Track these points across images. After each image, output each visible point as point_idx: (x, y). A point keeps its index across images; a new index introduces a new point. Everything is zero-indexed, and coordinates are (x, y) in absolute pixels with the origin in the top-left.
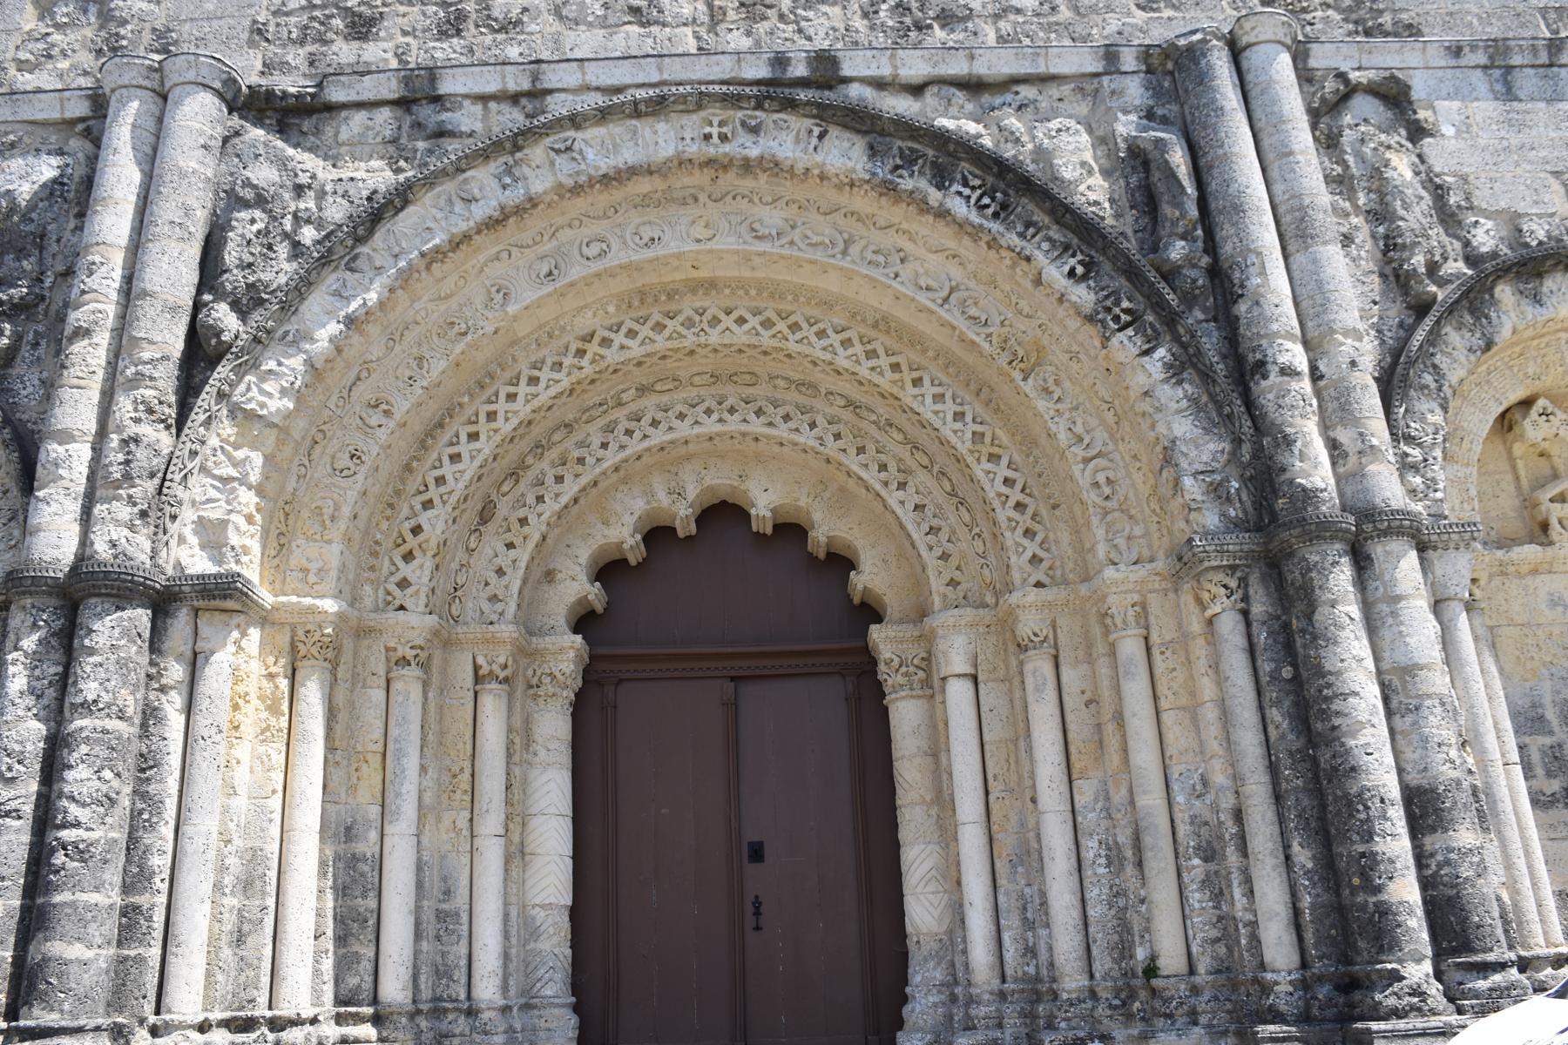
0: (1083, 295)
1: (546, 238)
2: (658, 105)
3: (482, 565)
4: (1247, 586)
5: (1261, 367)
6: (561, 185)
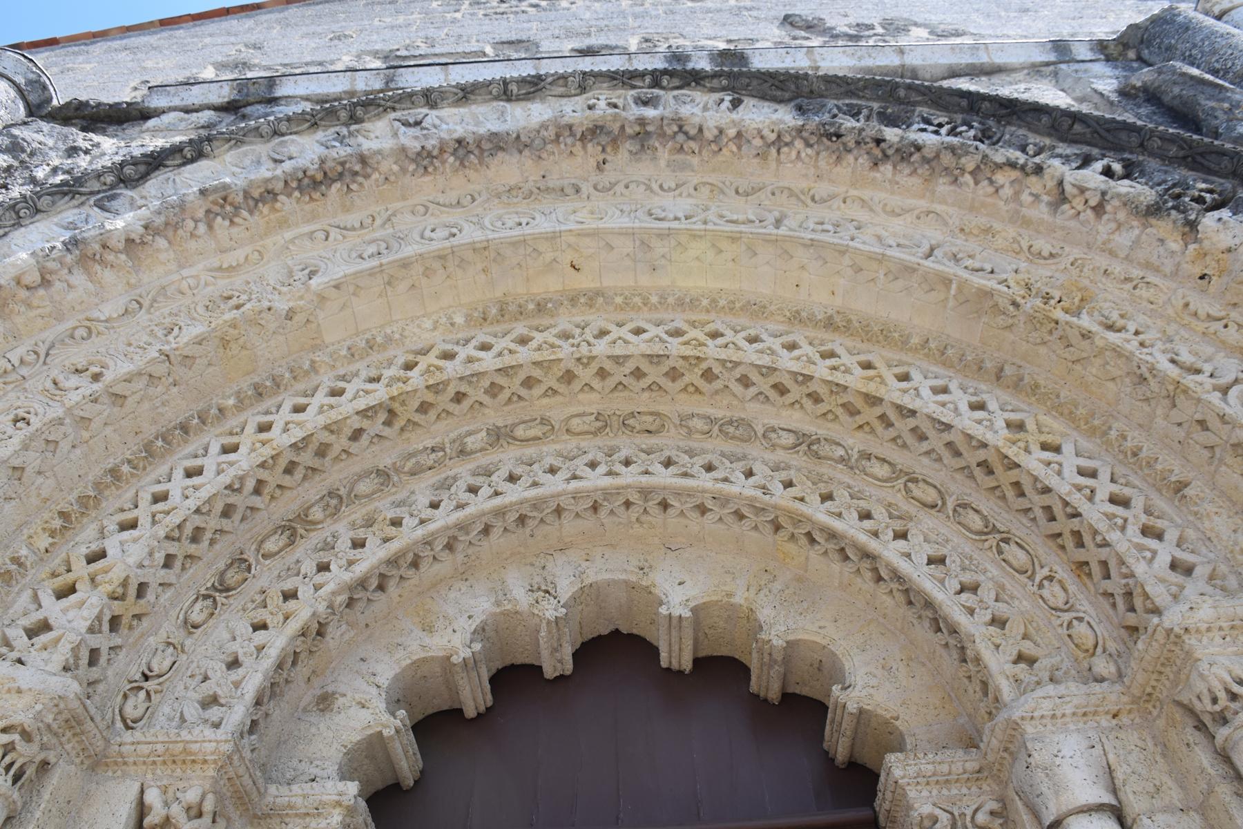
0: (1141, 191)
1: (378, 222)
3: (205, 652)
6: (403, 149)
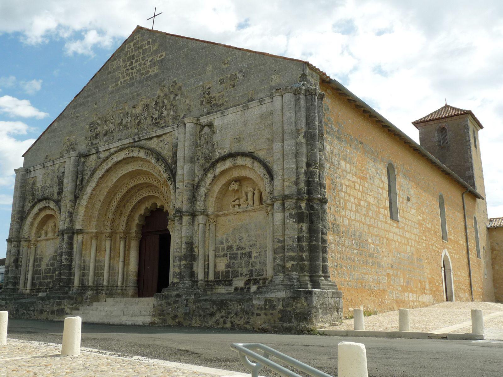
2: (121, 150)
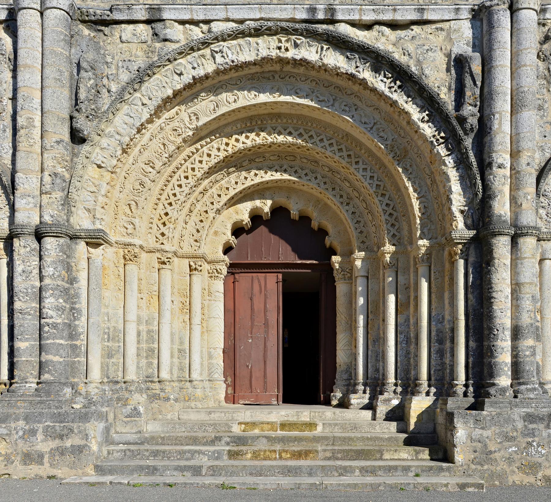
4: (469, 250)
5: (490, 165)
